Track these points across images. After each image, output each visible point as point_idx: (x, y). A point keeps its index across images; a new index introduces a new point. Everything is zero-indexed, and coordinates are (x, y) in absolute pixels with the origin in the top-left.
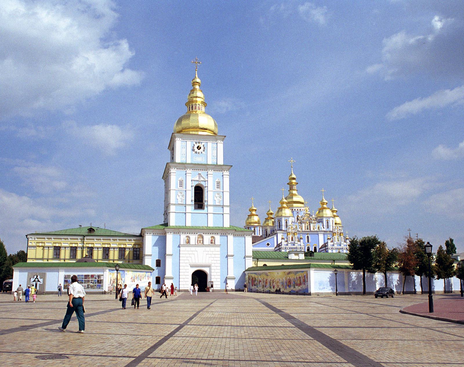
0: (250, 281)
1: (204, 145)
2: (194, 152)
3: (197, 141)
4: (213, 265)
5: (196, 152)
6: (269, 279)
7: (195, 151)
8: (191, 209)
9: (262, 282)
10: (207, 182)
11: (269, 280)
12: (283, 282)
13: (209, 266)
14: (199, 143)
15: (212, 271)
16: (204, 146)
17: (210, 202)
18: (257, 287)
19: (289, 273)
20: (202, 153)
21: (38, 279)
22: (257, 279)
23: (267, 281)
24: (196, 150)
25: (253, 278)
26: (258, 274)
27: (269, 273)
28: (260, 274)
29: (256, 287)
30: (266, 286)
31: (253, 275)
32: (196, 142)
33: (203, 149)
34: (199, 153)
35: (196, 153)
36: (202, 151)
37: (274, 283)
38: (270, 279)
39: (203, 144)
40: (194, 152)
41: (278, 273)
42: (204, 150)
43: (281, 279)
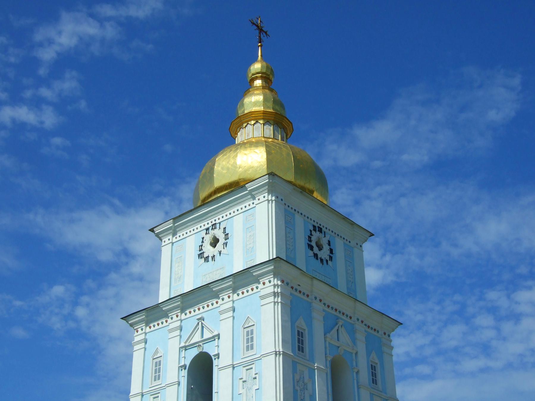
1: (329, 242)
2: (311, 253)
3: (315, 224)
5: (316, 255)
10: (354, 355)
14: (320, 230)
16: (329, 244)
20: (327, 261)
24: (316, 249)
32: (314, 226)
33: (328, 252)
34: (322, 260)
35: (317, 259)
36: (328, 258)
40: (311, 253)
42: (331, 258)
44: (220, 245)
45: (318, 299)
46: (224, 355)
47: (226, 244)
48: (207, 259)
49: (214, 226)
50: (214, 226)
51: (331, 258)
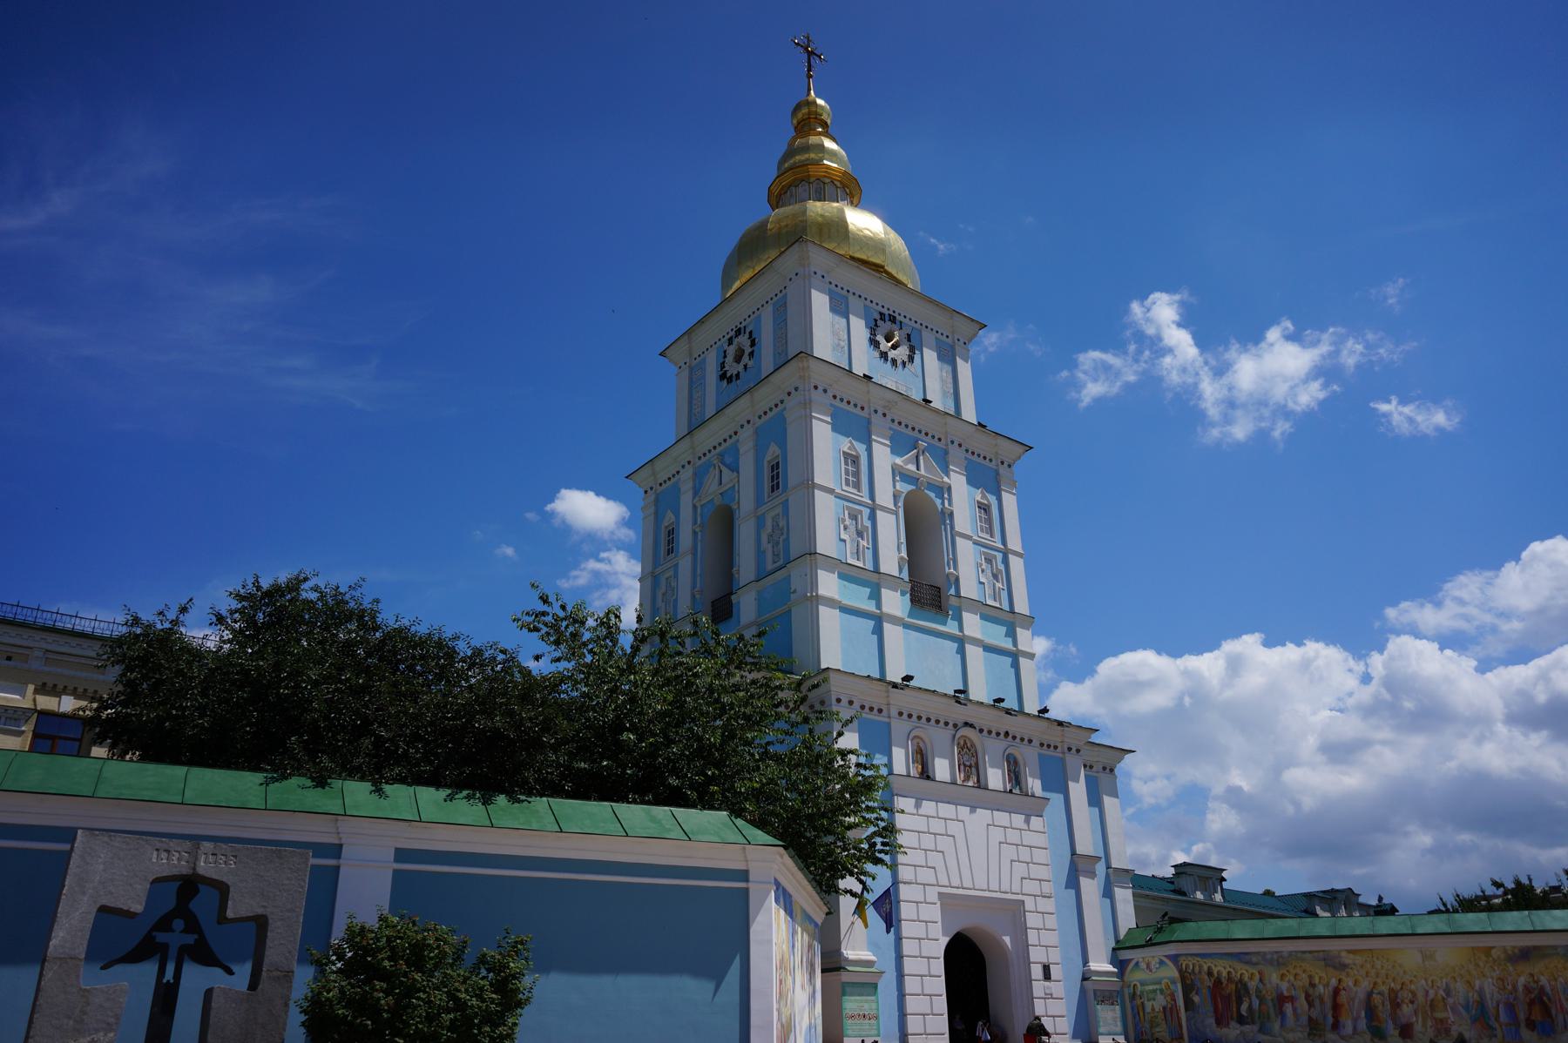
0: (1196, 999)
2: (877, 354)
4: (1029, 904)
6: (1357, 987)
7: (882, 348)
8: (895, 603)
9: (1302, 1003)
11: (1362, 995)
12: (1481, 1004)
13: (1014, 911)
15: (1032, 937)
17: (969, 589)
18: (1261, 1030)
19: (1525, 955)
21: (193, 925)
22: (1252, 985)
23: (1343, 998)
25: (1218, 982)
26: (1254, 959)
27: (1349, 952)
28: (1279, 961)
29: (1247, 1028)
30: (1336, 1026)
31: (1221, 968)
34: (894, 362)
37: (1407, 1009)
38: (1365, 985)
39: (907, 330)
41: (1427, 956)
43: (1460, 987)
44: (745, 359)
45: (880, 413)
46: (746, 502)
47: (751, 354)
48: (730, 380)
49: (738, 332)
50: (738, 332)
51: (911, 359)
